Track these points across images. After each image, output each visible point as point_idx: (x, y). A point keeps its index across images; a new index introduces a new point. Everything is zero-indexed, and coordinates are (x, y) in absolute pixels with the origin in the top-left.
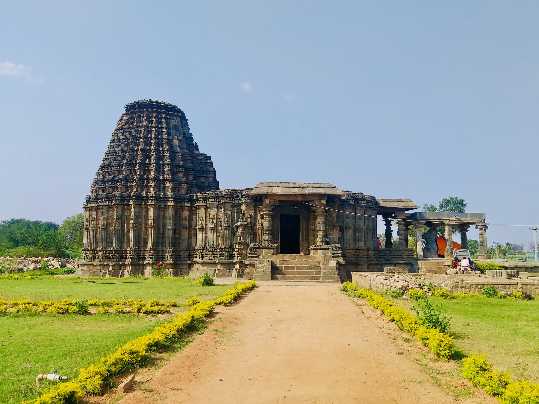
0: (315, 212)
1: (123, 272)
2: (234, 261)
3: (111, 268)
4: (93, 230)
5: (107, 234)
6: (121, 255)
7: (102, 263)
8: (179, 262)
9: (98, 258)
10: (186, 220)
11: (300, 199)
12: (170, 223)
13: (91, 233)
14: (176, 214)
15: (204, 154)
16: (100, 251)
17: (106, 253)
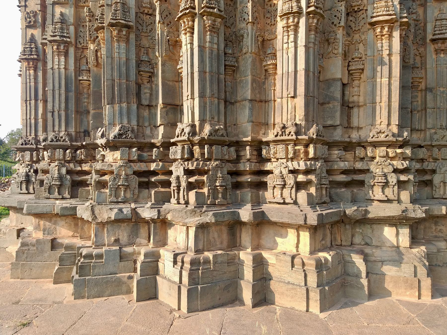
1: (260, 263)
3: (180, 237)
4: (63, 45)
5: (139, 63)
6: (234, 170)
7: (127, 209)
9: (101, 185)
13: (56, 62)
16: (112, 146)
17: (140, 160)
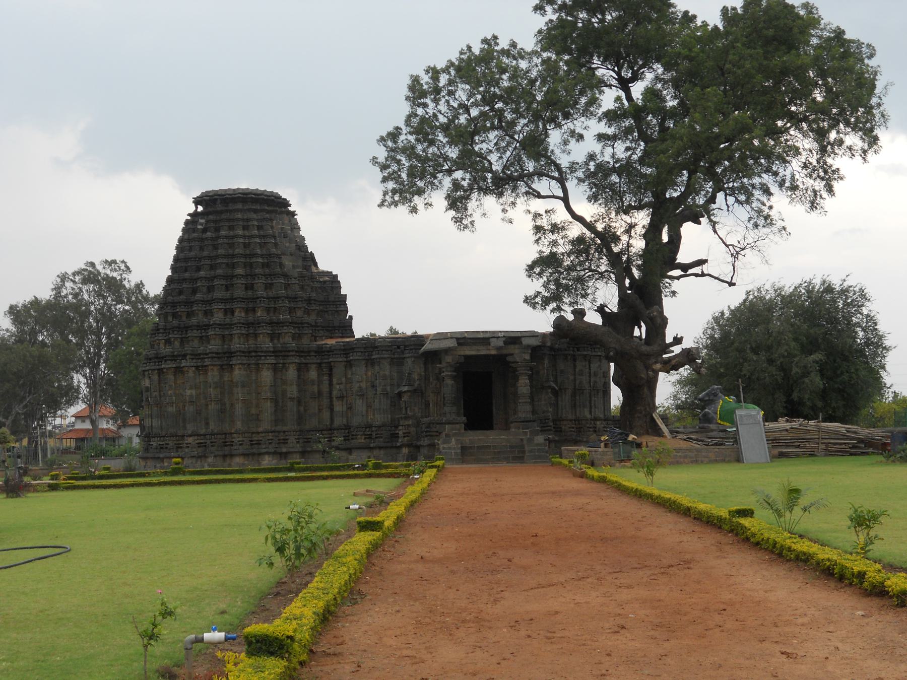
0: (515, 370)
2: (398, 444)
8: (309, 449)
10: (313, 384)
11: (481, 336)
12: (293, 390)
14: (299, 376)
15: (328, 272)
